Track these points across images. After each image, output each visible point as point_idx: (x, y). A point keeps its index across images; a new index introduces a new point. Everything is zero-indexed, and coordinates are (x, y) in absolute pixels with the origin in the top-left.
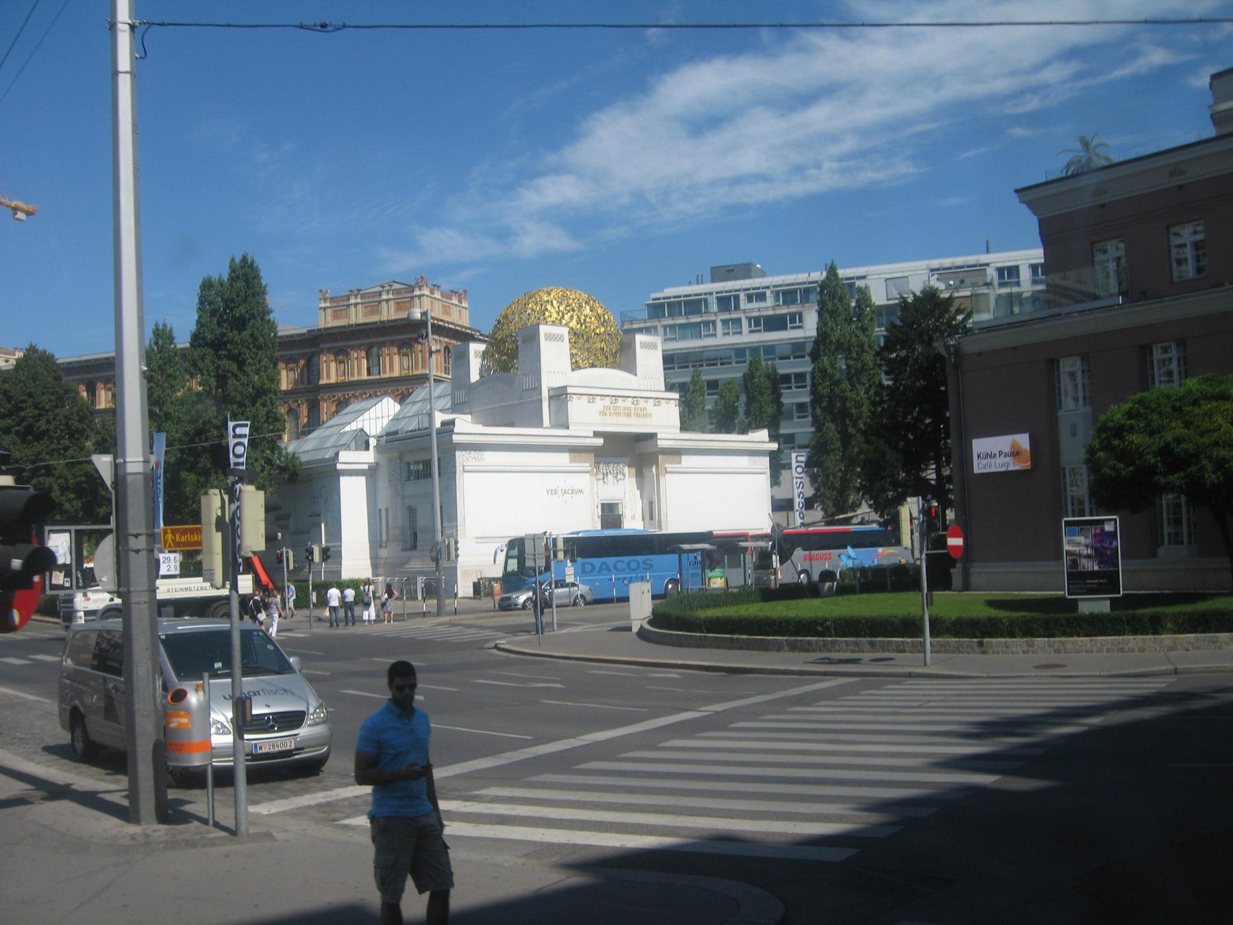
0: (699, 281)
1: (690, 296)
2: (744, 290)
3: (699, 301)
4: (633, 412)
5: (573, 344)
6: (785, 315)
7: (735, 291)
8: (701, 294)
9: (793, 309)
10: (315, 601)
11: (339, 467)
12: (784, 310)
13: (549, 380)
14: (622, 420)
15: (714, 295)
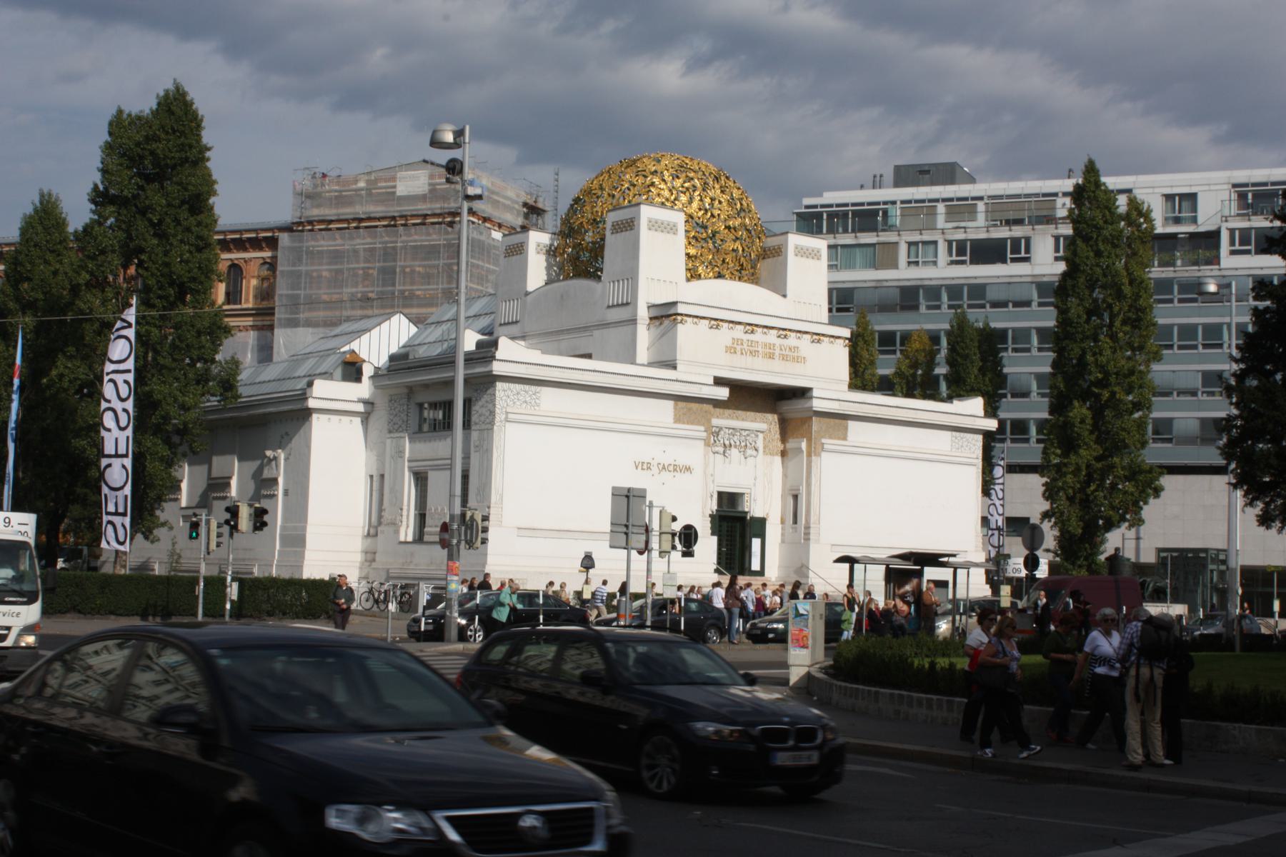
0: (877, 183)
1: (862, 204)
2: (944, 200)
3: (875, 213)
4: (777, 352)
5: (692, 240)
6: (1005, 240)
7: (930, 201)
8: (878, 203)
9: (1018, 231)
10: (235, 597)
11: (312, 403)
12: (1003, 233)
13: (650, 292)
14: (759, 362)
15: (898, 205)
